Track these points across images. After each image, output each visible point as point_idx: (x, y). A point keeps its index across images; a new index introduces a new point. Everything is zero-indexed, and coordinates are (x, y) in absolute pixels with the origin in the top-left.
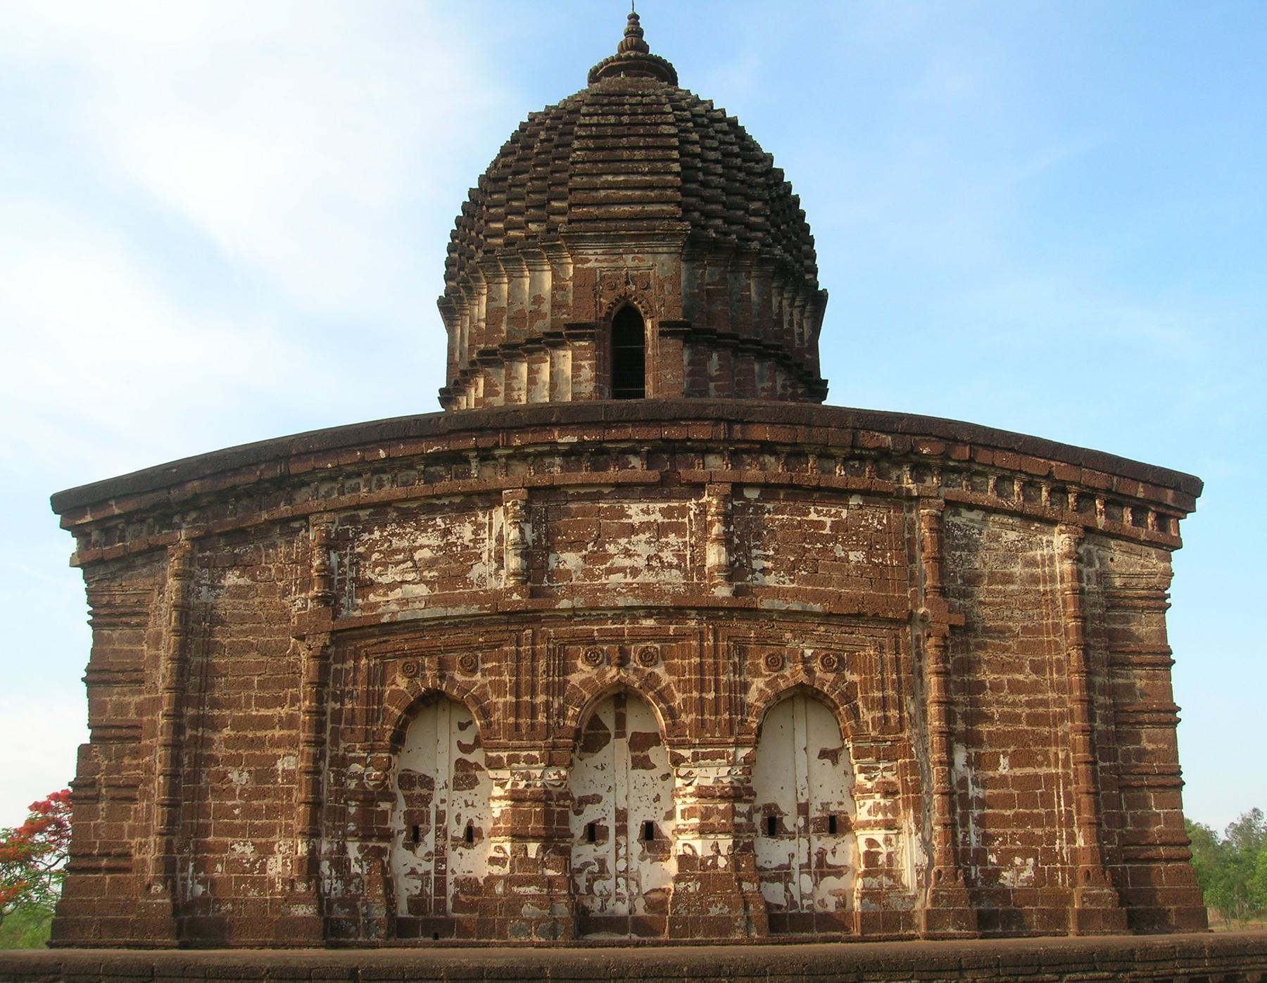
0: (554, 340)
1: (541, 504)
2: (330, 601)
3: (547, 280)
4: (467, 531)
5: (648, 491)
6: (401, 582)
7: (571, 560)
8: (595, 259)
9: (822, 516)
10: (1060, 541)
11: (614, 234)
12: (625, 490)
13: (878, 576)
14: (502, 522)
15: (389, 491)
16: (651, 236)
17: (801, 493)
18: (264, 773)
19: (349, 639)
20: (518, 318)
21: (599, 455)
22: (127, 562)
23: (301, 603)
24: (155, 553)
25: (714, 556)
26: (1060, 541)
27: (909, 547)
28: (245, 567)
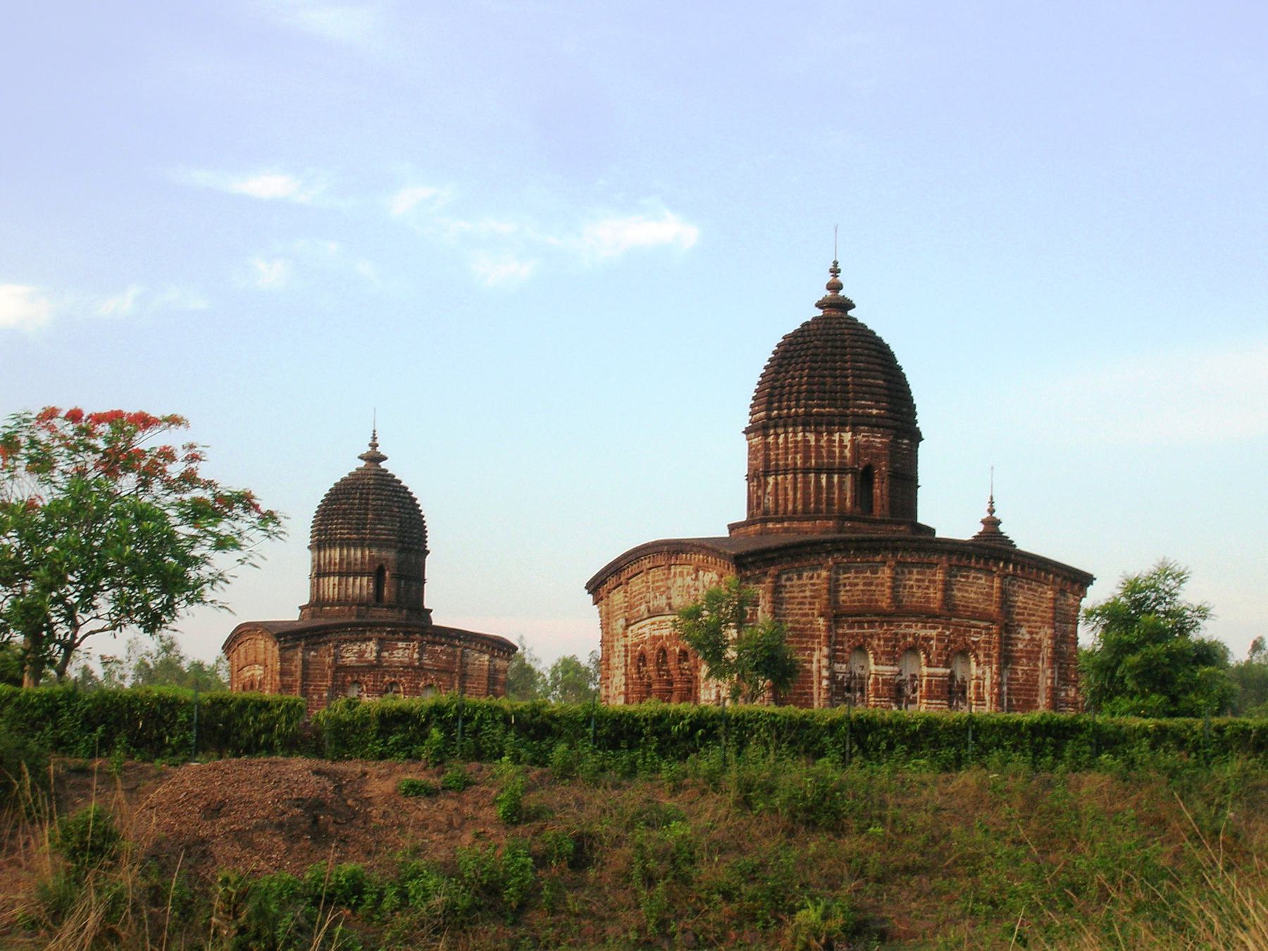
0: (362, 575)
1: (381, 642)
2: (335, 660)
3: (359, 554)
4: (364, 646)
5: (403, 640)
6: (350, 656)
7: (386, 654)
8: (375, 552)
9: (438, 648)
10: (487, 657)
11: (381, 545)
12: (399, 640)
13: (448, 662)
14: (372, 646)
15: (348, 636)
16: (390, 546)
17: (434, 643)
18: (320, 696)
19: (339, 669)
20: (349, 564)
21: (394, 633)
22: (289, 648)
23: (329, 660)
24: (296, 646)
25: (416, 656)
26: (487, 657)
27: (455, 656)
28: (316, 651)
